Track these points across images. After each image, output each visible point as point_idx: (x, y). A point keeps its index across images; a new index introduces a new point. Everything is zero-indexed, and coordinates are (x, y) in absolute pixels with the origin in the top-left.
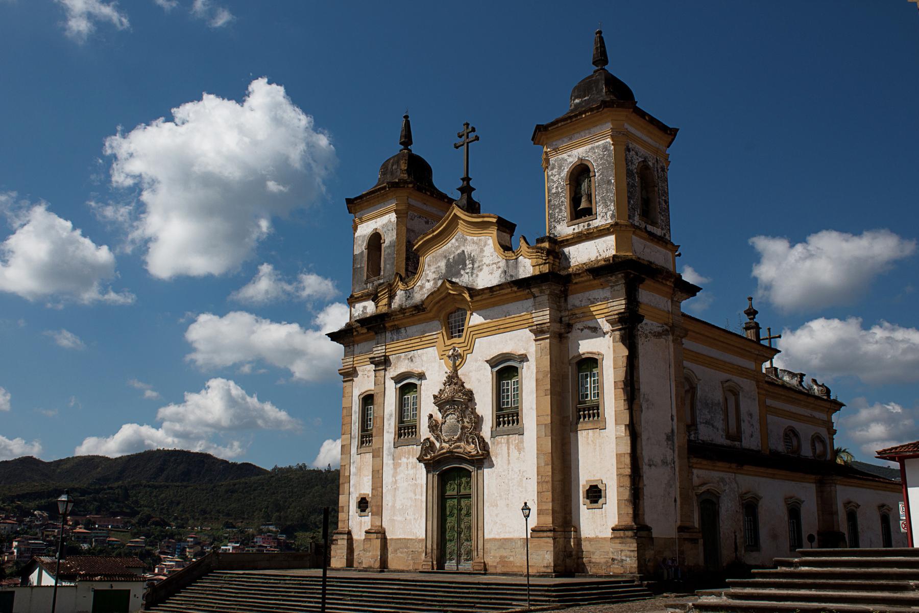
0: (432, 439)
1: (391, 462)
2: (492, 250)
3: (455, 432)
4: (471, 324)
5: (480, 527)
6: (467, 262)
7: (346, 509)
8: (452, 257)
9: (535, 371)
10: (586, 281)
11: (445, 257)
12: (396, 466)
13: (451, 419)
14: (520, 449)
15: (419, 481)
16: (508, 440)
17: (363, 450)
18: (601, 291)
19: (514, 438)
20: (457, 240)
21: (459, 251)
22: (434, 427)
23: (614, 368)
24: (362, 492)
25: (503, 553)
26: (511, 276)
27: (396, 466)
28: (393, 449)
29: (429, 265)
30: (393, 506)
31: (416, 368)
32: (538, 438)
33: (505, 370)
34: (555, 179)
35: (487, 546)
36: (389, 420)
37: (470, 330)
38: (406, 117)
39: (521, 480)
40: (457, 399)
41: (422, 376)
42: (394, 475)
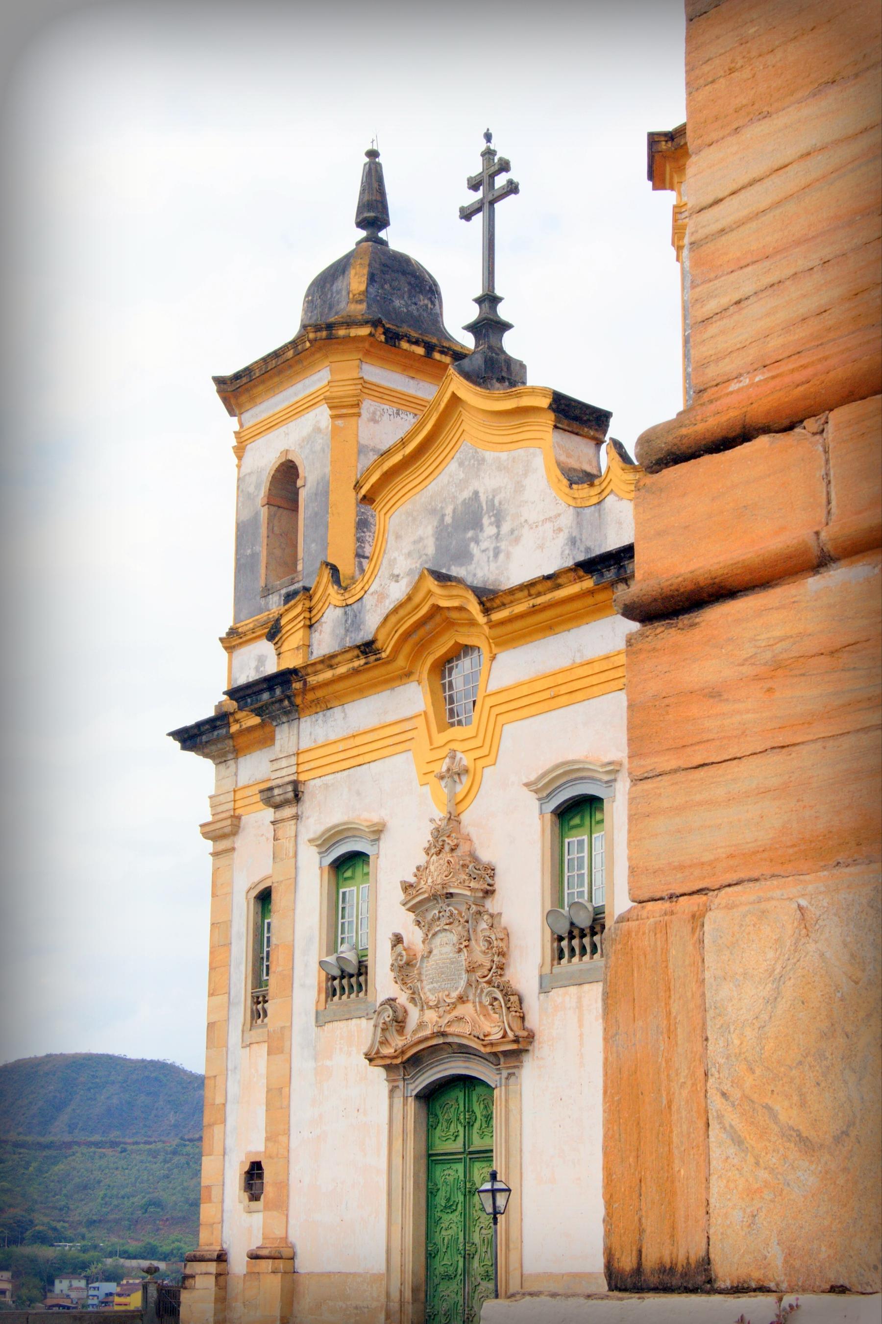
0: (403, 999)
4: (493, 686)
6: (486, 521)
7: (215, 1192)
8: (449, 511)
13: (445, 945)
16: (580, 998)
20: (461, 464)
21: (466, 494)
22: (405, 969)
29: (398, 537)
31: (368, 816)
37: (490, 702)
41: (378, 832)
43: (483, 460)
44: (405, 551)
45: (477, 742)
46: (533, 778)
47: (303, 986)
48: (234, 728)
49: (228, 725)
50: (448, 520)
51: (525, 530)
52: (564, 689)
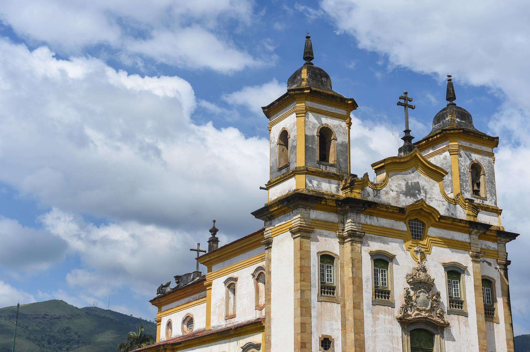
1: (371, 315)
2: (439, 191)
6: (422, 191)
7: (307, 345)
10: (491, 235)
11: (405, 180)
12: (375, 319)
15: (395, 334)
18: (492, 243)
19: (462, 318)
21: (415, 181)
22: (408, 298)
23: (502, 290)
24: (325, 333)
26: (452, 214)
27: (375, 319)
28: (371, 306)
32: (478, 321)
33: (454, 273)
34: (463, 164)
36: (367, 282)
38: (308, 37)
39: (468, 347)
40: (421, 283)
43: (420, 175)
44: (396, 185)
45: (427, 247)
46: (447, 262)
47: (366, 292)
48: (323, 202)
49: (321, 201)
50: (410, 184)
51: (434, 200)
52: (451, 244)
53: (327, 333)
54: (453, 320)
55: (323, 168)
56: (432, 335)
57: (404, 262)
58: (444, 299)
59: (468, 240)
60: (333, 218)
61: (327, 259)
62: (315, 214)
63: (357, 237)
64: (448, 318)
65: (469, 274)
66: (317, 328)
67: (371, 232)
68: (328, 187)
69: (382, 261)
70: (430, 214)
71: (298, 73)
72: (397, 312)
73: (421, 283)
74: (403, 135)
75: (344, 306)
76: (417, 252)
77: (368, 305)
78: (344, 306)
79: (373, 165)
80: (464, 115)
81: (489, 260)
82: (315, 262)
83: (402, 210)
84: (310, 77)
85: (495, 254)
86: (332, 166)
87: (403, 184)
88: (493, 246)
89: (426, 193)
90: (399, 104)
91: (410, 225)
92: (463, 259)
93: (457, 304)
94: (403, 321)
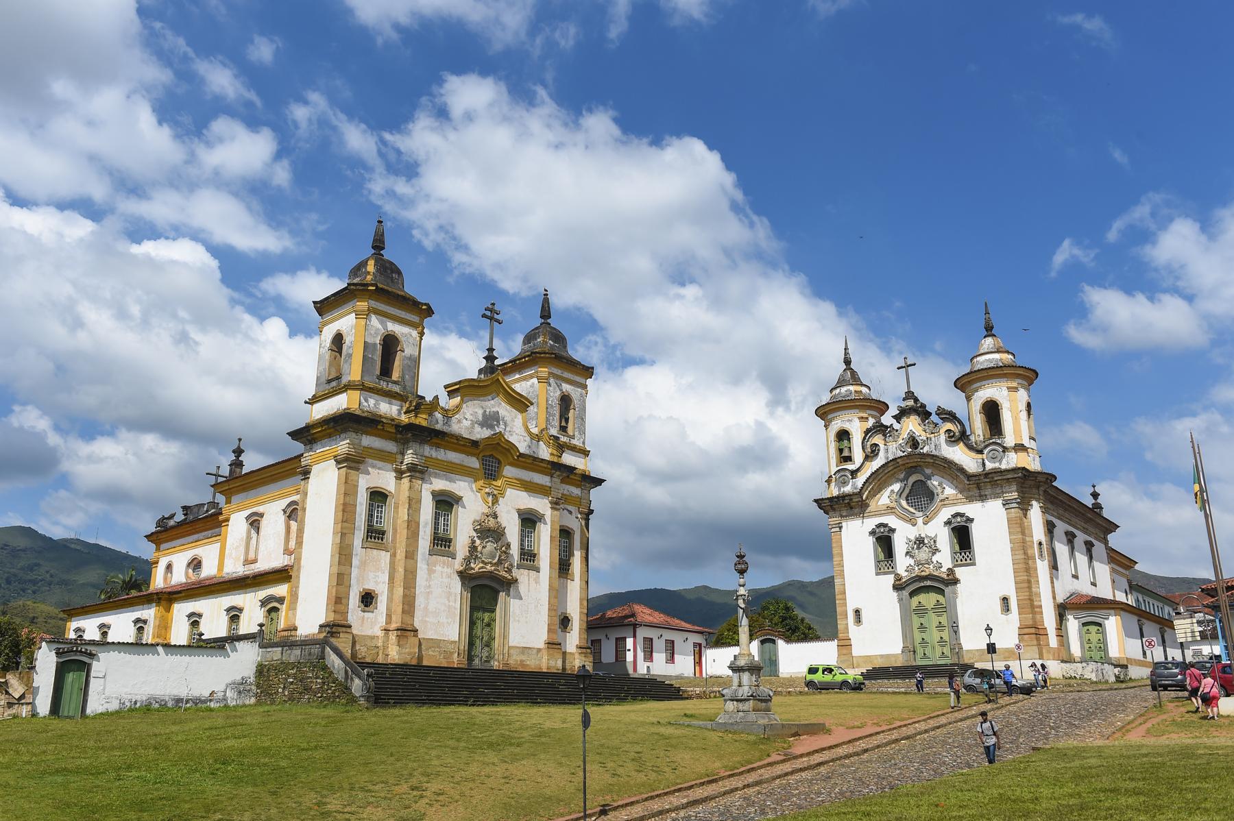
3: (494, 558)
5: (505, 636)
9: (549, 527)
12: (431, 571)
14: (537, 581)
17: (368, 545)
19: (533, 573)
22: (473, 548)
24: (367, 587)
25: (523, 658)
27: (431, 571)
30: (426, 608)
33: (529, 520)
35: (512, 651)
40: (489, 532)
42: (429, 579)
53: (370, 586)
54: (523, 576)
55: (383, 385)
56: (497, 592)
57: (473, 503)
58: (515, 551)
59: (549, 484)
60: (391, 446)
61: (378, 497)
62: (368, 441)
63: (417, 472)
64: (516, 573)
65: (545, 523)
66: (358, 580)
67: (435, 467)
68: (388, 409)
69: (446, 503)
70: (508, 450)
71: (364, 264)
72: (458, 564)
73: (489, 532)
74: (486, 354)
75: (393, 555)
76: (488, 494)
77: (423, 554)
78: (393, 555)
79: (446, 387)
80: (558, 337)
81: (570, 508)
82: (362, 499)
83: (475, 443)
84: (378, 270)
85: (577, 501)
86: (395, 382)
87: (480, 412)
88: (576, 491)
89: (506, 425)
90: (484, 316)
91: (484, 461)
92: (541, 505)
93: (528, 557)
94: (463, 575)
